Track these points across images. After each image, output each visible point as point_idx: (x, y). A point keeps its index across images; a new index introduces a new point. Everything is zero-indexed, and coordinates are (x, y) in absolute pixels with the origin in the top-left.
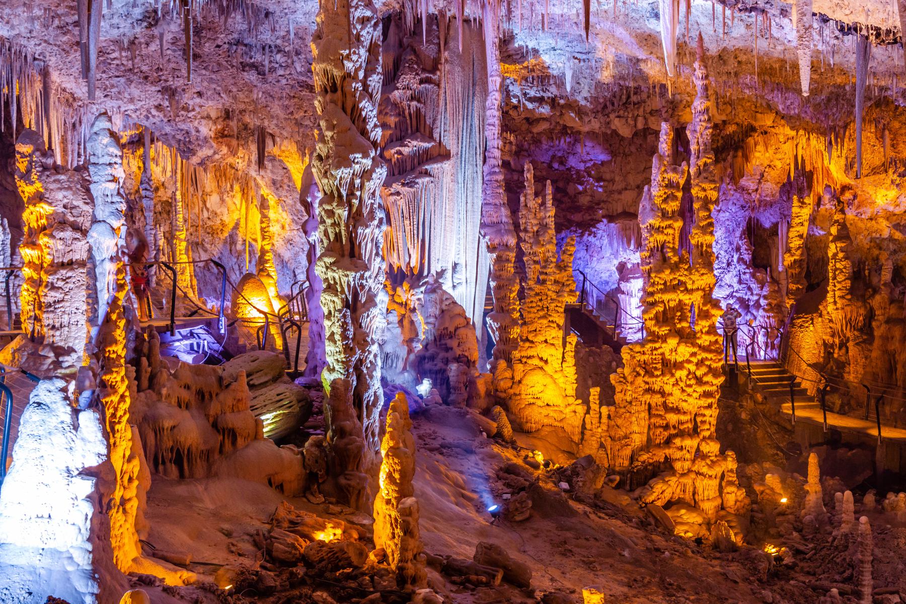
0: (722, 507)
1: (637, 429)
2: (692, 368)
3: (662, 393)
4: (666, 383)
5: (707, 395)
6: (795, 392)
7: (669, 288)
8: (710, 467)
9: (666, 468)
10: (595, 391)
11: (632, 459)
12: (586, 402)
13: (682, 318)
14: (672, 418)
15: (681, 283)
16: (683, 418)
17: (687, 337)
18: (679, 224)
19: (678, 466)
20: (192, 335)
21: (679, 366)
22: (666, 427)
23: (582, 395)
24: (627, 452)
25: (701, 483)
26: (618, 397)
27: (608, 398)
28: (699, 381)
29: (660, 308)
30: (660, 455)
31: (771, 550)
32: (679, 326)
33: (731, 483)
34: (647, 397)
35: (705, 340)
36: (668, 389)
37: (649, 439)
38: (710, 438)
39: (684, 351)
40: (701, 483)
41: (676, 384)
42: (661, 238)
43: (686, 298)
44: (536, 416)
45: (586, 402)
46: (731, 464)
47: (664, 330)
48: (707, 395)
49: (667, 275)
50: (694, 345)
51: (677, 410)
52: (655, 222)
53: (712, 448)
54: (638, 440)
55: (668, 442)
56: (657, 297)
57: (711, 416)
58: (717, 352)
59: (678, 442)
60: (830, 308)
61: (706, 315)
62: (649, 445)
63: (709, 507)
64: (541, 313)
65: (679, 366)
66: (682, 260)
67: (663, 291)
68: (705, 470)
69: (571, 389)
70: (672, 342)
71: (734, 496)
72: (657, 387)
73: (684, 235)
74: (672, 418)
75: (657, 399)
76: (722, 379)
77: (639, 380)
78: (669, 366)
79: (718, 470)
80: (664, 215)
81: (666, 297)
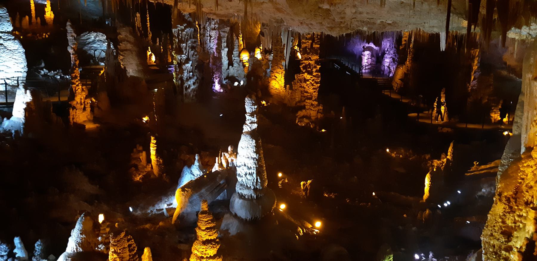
0: (317, 118)
1: (298, 97)
4: (304, 85)
5: (314, 89)
6: (391, 88)
7: (306, 59)
9: (304, 107)
11: (296, 104)
12: (286, 89)
13: (310, 68)
15: (310, 58)
17: (310, 73)
18: (310, 41)
19: (306, 107)
21: (308, 80)
22: (304, 97)
23: (285, 86)
24: (294, 102)
25: (312, 112)
26: (293, 88)
27: (291, 88)
28: (313, 85)
31: (323, 130)
33: (320, 113)
35: (314, 74)
36: (305, 86)
37: (301, 99)
38: (315, 100)
40: (312, 112)
41: (307, 85)
43: (311, 62)
44: (273, 91)
45: (286, 89)
46: (321, 108)
47: (304, 71)
48: (314, 89)
50: (312, 75)
51: (307, 92)
53: (316, 103)
54: (297, 99)
55: (305, 100)
57: (316, 94)
58: (318, 77)
60: (408, 63)
61: (315, 67)
62: (299, 102)
63: (313, 118)
65: (308, 80)
66: (310, 52)
67: (304, 60)
69: (283, 85)
70: (306, 74)
71: (319, 116)
73: (312, 44)
75: (303, 89)
76: (319, 85)
77: (298, 84)
78: (306, 80)
79: (317, 109)
80: (307, 39)
81: (305, 62)
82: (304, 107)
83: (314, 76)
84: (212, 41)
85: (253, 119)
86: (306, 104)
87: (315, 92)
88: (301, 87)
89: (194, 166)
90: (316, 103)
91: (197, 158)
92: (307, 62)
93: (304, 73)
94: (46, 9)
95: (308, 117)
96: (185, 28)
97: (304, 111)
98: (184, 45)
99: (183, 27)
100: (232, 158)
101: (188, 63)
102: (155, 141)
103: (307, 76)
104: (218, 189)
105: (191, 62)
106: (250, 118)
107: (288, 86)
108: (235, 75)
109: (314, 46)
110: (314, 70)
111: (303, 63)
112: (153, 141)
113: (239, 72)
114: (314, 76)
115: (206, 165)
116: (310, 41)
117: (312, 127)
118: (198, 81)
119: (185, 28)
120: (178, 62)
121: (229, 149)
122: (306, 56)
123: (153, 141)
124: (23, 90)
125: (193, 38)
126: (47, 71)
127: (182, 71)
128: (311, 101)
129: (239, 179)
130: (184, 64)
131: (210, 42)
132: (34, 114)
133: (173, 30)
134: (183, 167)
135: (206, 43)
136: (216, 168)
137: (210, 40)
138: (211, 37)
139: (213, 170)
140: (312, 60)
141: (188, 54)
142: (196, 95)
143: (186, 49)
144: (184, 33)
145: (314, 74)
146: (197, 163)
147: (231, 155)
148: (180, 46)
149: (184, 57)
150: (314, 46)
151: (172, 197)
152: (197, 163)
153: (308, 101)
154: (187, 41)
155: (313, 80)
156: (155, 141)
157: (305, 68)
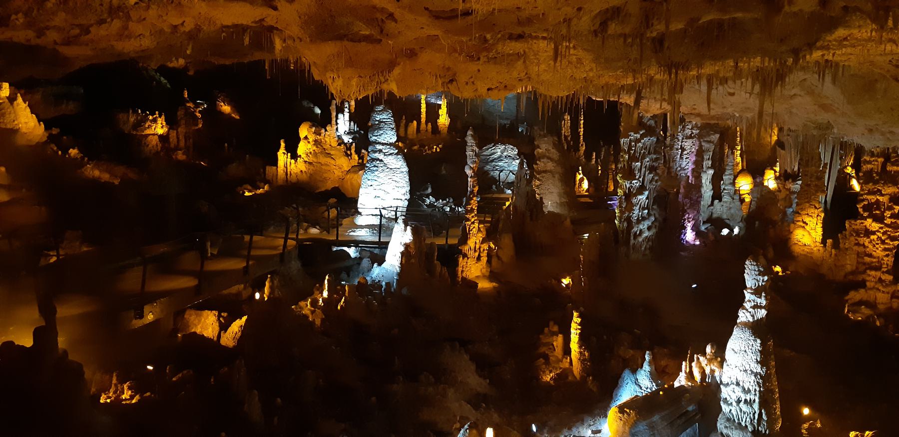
1: (850, 262)
2: (880, 235)
4: (866, 241)
5: (885, 250)
7: (870, 193)
8: (884, 287)
9: (862, 285)
10: (829, 241)
11: (845, 276)
12: (825, 246)
13: (878, 208)
14: (867, 259)
17: (879, 219)
18: (881, 160)
19: (868, 284)
21: (874, 233)
22: (864, 264)
23: (824, 242)
24: (842, 273)
26: (841, 245)
27: (836, 245)
28: (883, 242)
30: (860, 278)
34: (856, 248)
35: (888, 221)
36: (866, 244)
37: (857, 268)
38: (887, 272)
39: (875, 226)
41: (871, 242)
42: (870, 166)
43: (881, 198)
44: (797, 249)
45: (825, 246)
47: (866, 214)
48: (885, 250)
51: (870, 256)
52: (868, 159)
54: (849, 268)
55: (864, 272)
57: (889, 261)
59: (868, 272)
61: (890, 208)
62: (853, 273)
65: (874, 233)
66: (881, 179)
67: (867, 194)
68: (880, 288)
70: (870, 220)
72: (861, 243)
73: (884, 166)
74: (867, 259)
75: (861, 249)
77: (852, 238)
78: (868, 233)
79: (891, 289)
80: (872, 154)
81: (869, 197)
82: (862, 285)
83: (887, 225)
84: (685, 157)
85: (759, 300)
86: (868, 278)
87: (887, 256)
88: (858, 244)
89: (642, 372)
90: (890, 278)
91: (647, 357)
92: (872, 198)
94: (440, 111)
95: (871, 305)
96: (642, 136)
97: (862, 291)
98: (639, 164)
99: (639, 136)
100: (713, 367)
101: (642, 194)
102: (579, 320)
104: (683, 420)
105: (647, 193)
106: (753, 297)
107: (829, 241)
108: (725, 217)
109: (889, 168)
110: (888, 214)
111: (863, 200)
113: (732, 211)
114: (887, 225)
115: (662, 374)
116: (881, 160)
117: (878, 323)
118: (657, 224)
119: (642, 136)
120: (625, 192)
121: (709, 349)
122: (870, 186)
124: (403, 226)
125: (655, 154)
126: (434, 200)
127: (630, 207)
128: (878, 274)
129: (725, 408)
130: (635, 195)
131: (681, 158)
132: (413, 261)
133: (622, 141)
134: (622, 371)
135: (674, 161)
136: (681, 381)
137: (681, 155)
138: (683, 149)
139: (677, 384)
140: (882, 195)
141: (643, 180)
142: (651, 248)
143: (640, 170)
144: (640, 145)
145: (888, 221)
146: (646, 367)
147: (710, 361)
148: (630, 166)
149: (636, 183)
150: (889, 168)
151: (602, 420)
152: (646, 367)
153: (873, 273)
154: (644, 158)
155: (884, 233)
156: (579, 320)
157: (865, 208)
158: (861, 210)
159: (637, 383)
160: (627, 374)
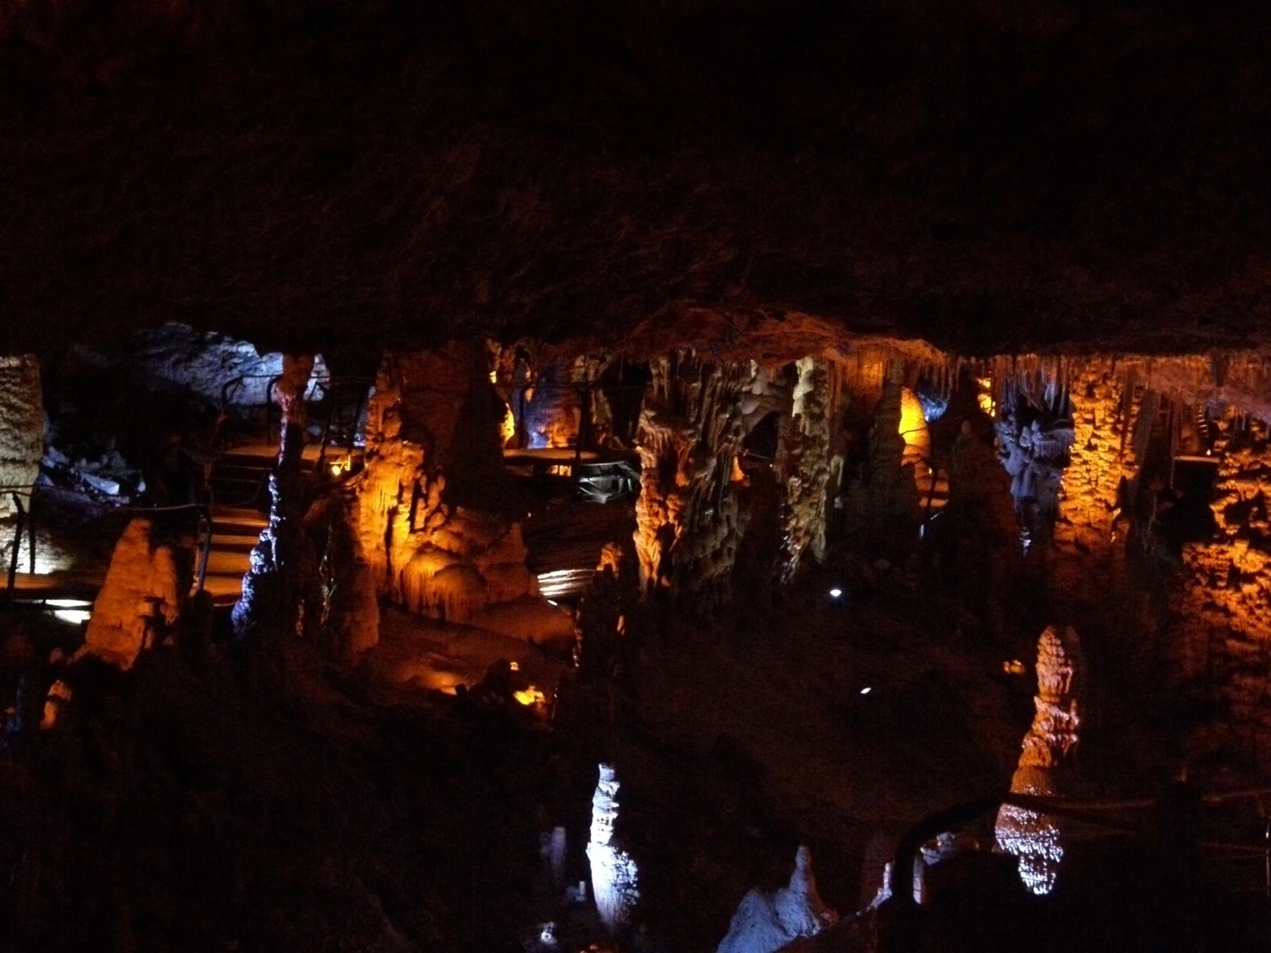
3: (1225, 609)
7: (1244, 475)
16: (1251, 648)
19: (1236, 709)
20: (617, 471)
21: (1250, 578)
22: (1227, 657)
29: (1233, 500)
32: (1252, 525)
36: (1233, 606)
41: (1242, 601)
49: (1245, 457)
51: (1242, 636)
56: (1231, 484)
64: (1086, 488)
65: (1250, 578)
67: (1238, 477)
72: (1221, 603)
75: (1220, 618)
77: (1198, 591)
78: (1237, 577)
81: (1241, 486)
85: (1066, 716)
89: (789, 896)
91: (801, 860)
92: (1249, 489)
93: (1231, 540)
102: (616, 786)
103: (1241, 554)
106: (1055, 711)
111: (1227, 492)
112: (607, 784)
118: (733, 545)
123: (607, 784)
124: (143, 547)
126: (63, 459)
132: (169, 641)
143: (700, 402)
146: (799, 884)
152: (799, 884)
156: (616, 786)
158: (1220, 518)
159: (776, 921)
160: (752, 902)
